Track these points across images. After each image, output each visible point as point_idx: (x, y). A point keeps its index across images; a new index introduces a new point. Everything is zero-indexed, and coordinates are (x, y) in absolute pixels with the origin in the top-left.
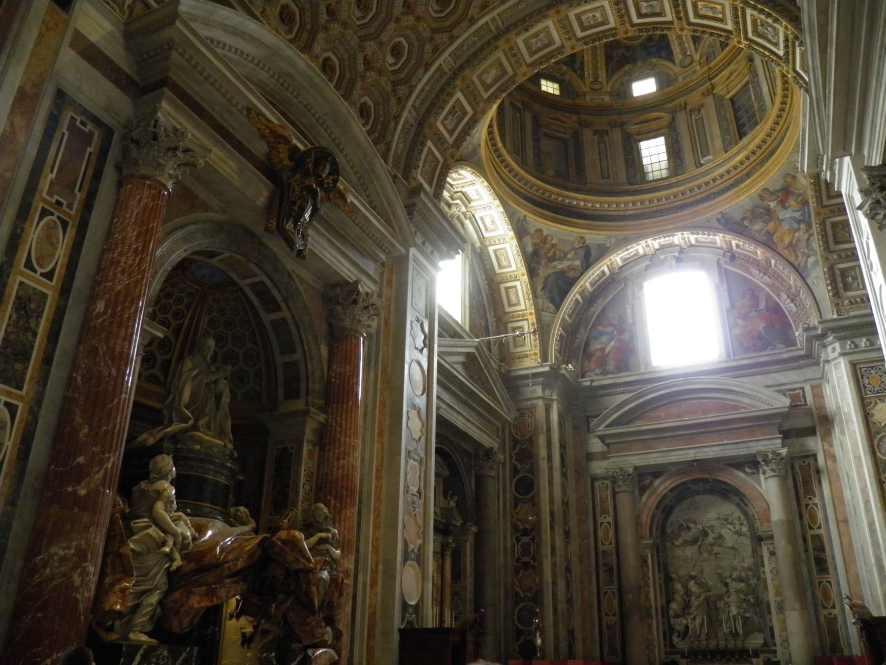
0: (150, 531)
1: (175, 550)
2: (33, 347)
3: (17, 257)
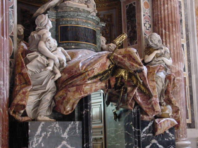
0: (38, 58)
1: (55, 68)
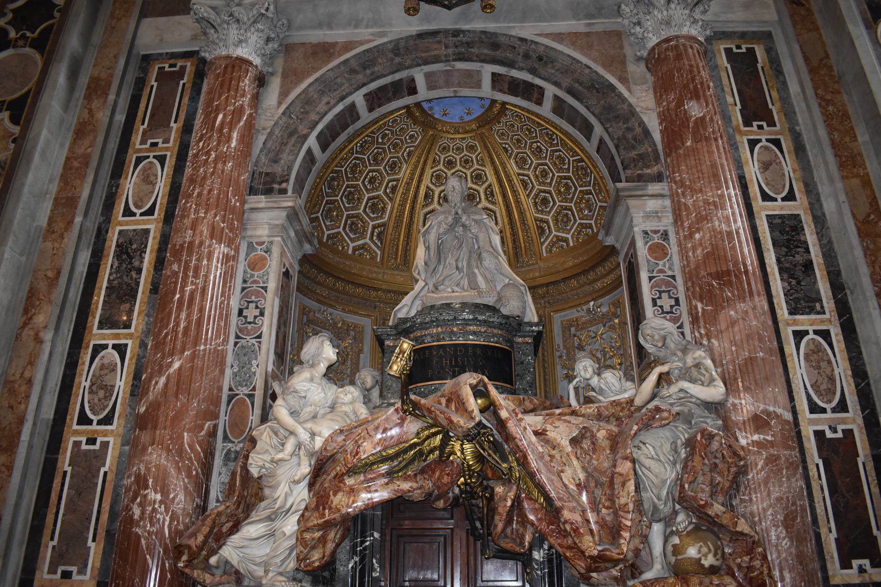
2: (138, 284)
3: (114, 211)
